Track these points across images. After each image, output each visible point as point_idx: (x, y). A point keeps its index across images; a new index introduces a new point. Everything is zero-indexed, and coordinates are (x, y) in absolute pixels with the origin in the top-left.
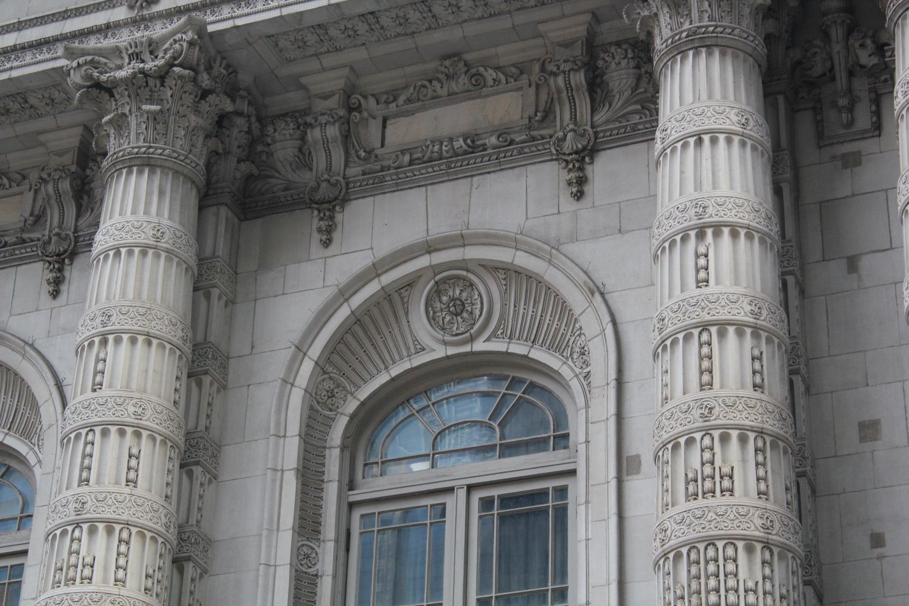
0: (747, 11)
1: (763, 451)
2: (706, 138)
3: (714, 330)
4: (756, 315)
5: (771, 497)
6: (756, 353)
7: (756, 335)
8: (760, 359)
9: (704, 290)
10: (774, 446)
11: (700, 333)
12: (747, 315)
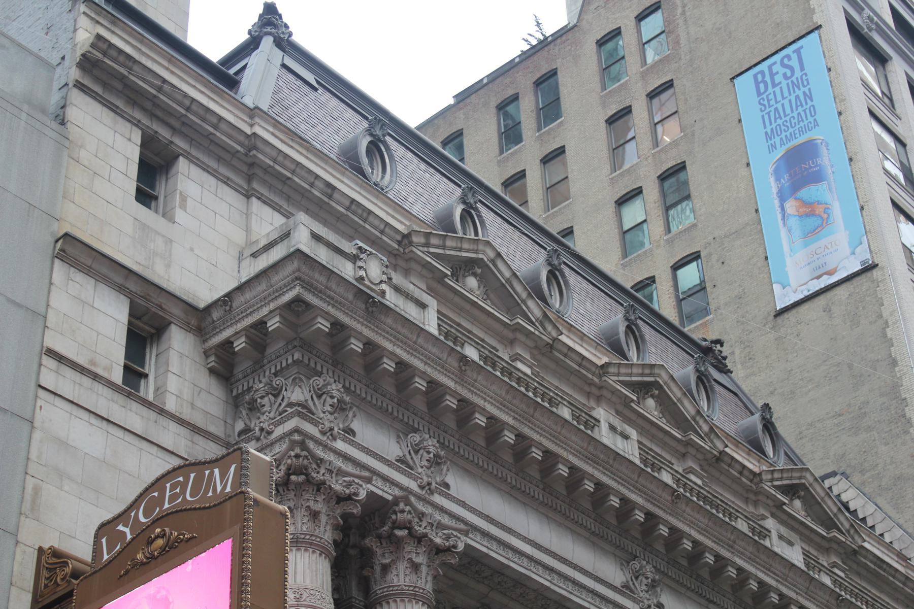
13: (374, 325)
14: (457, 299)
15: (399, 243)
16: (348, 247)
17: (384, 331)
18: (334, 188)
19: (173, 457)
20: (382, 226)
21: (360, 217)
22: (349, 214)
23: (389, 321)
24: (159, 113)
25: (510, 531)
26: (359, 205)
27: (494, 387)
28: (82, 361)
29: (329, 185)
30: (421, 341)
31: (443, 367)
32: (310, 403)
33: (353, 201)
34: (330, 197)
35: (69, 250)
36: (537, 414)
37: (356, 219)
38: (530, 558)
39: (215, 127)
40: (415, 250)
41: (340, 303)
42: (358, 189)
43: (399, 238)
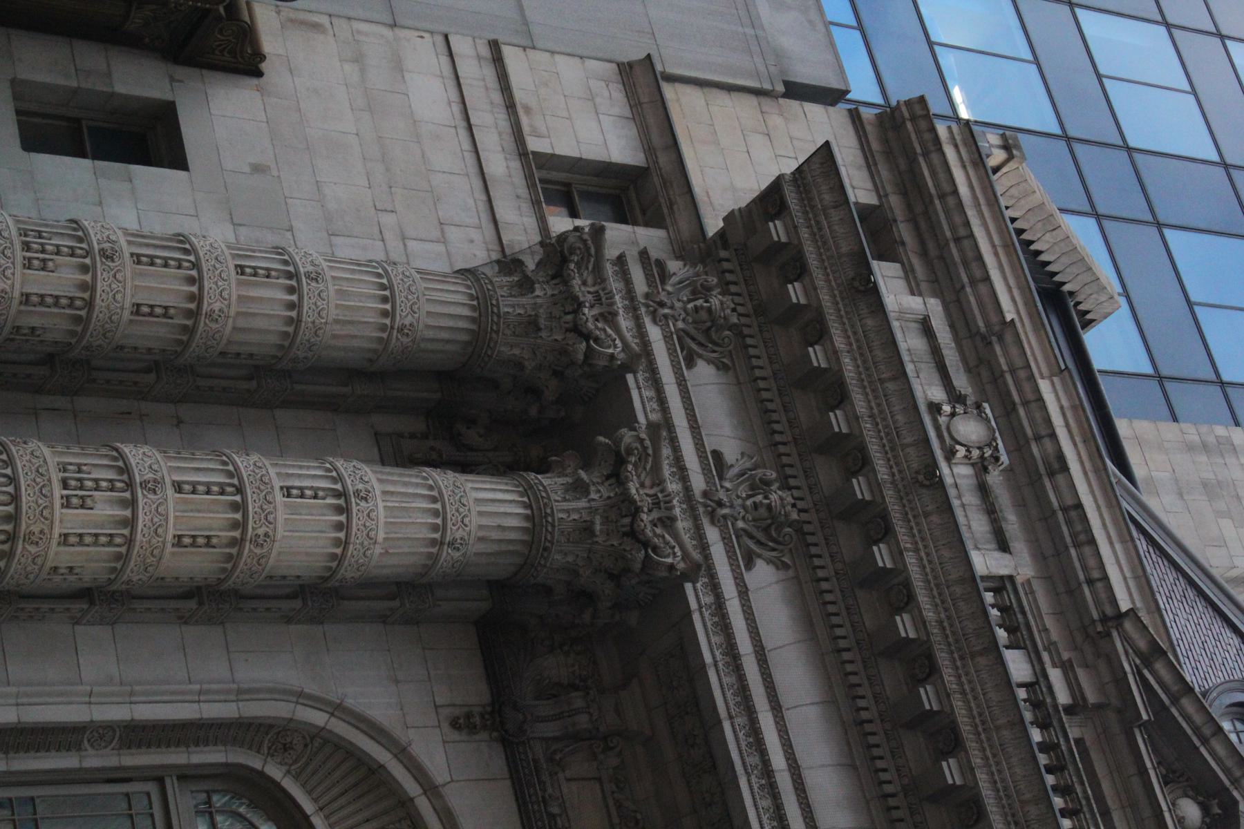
0: (516, 351)
1: (71, 306)
2: (387, 293)
3: (194, 273)
4: (209, 315)
5: (23, 308)
6: (172, 311)
7: (190, 314)
8: (165, 315)
9: (233, 273)
10: (77, 319)
11: (189, 261)
12: (209, 304)
13: (845, 306)
14: (1136, 782)
15: (1105, 619)
16: (961, 382)
17: (852, 326)
18: (1065, 468)
19: (491, 226)
20: (1096, 574)
21: (1074, 536)
22: (1060, 515)
23: (870, 322)
24: (923, 225)
25: (776, 707)
26: (1084, 518)
27: (946, 553)
28: (519, 95)
29: (1061, 457)
30: (891, 386)
31: (892, 449)
32: (674, 279)
33: (1079, 506)
34: (1051, 474)
35: (638, 71)
36: (982, 661)
37: (1064, 528)
38: (767, 771)
39: (973, 282)
40: (1115, 634)
41: (825, 243)
42: (1128, 575)
43: (1109, 611)
